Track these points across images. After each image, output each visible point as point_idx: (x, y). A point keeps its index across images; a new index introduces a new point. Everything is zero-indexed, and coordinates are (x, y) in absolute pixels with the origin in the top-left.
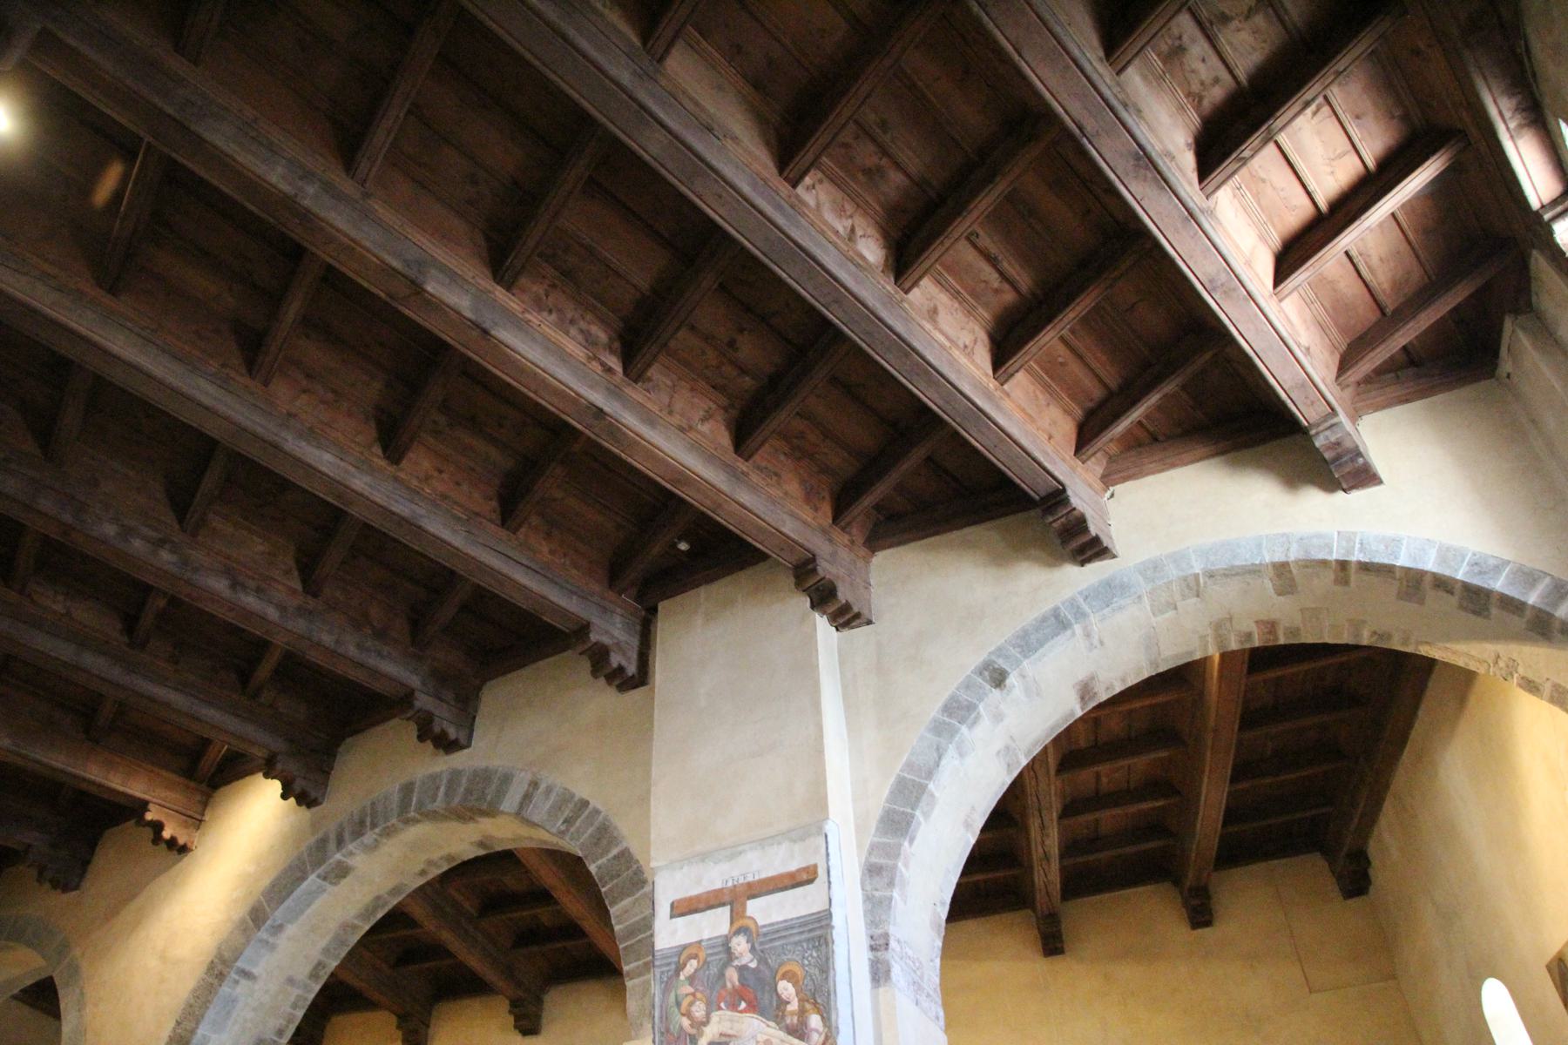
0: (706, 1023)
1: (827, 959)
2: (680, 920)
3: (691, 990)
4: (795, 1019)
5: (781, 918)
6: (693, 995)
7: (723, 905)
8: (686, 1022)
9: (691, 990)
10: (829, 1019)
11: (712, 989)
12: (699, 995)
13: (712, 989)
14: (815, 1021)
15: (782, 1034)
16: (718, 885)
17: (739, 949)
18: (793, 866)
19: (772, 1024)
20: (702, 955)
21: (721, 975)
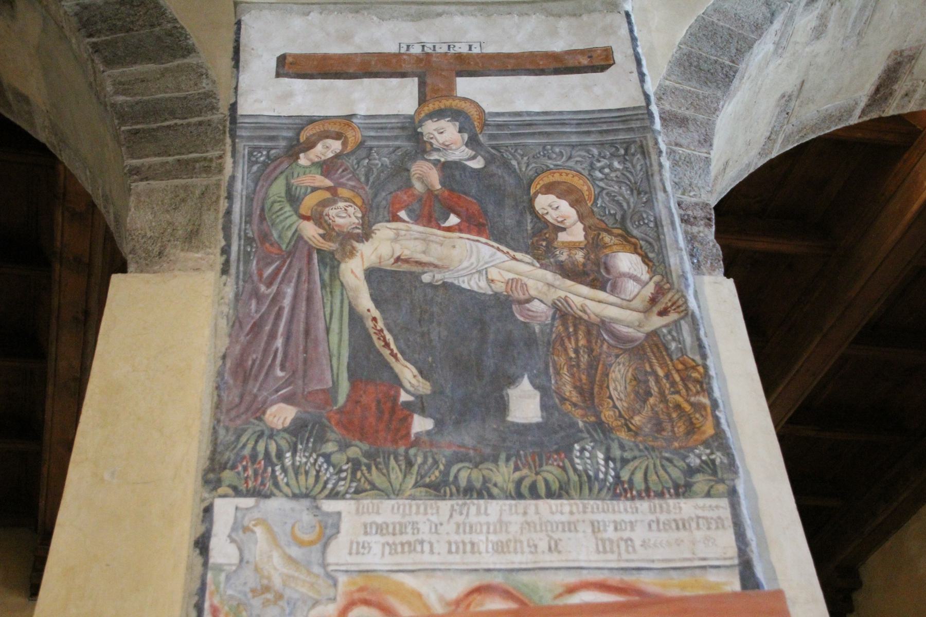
0: (366, 235)
1: (648, 176)
2: (299, 84)
3: (328, 183)
4: (579, 256)
5: (537, 109)
6: (332, 190)
7: (403, 75)
8: (310, 231)
9: (328, 183)
10: (664, 261)
11: (378, 188)
12: (344, 192)
13: (378, 188)
14: (627, 262)
15: (549, 276)
16: (390, 47)
17: (441, 138)
18: (558, 46)
19: (528, 258)
20: (353, 137)
21: (401, 170)
